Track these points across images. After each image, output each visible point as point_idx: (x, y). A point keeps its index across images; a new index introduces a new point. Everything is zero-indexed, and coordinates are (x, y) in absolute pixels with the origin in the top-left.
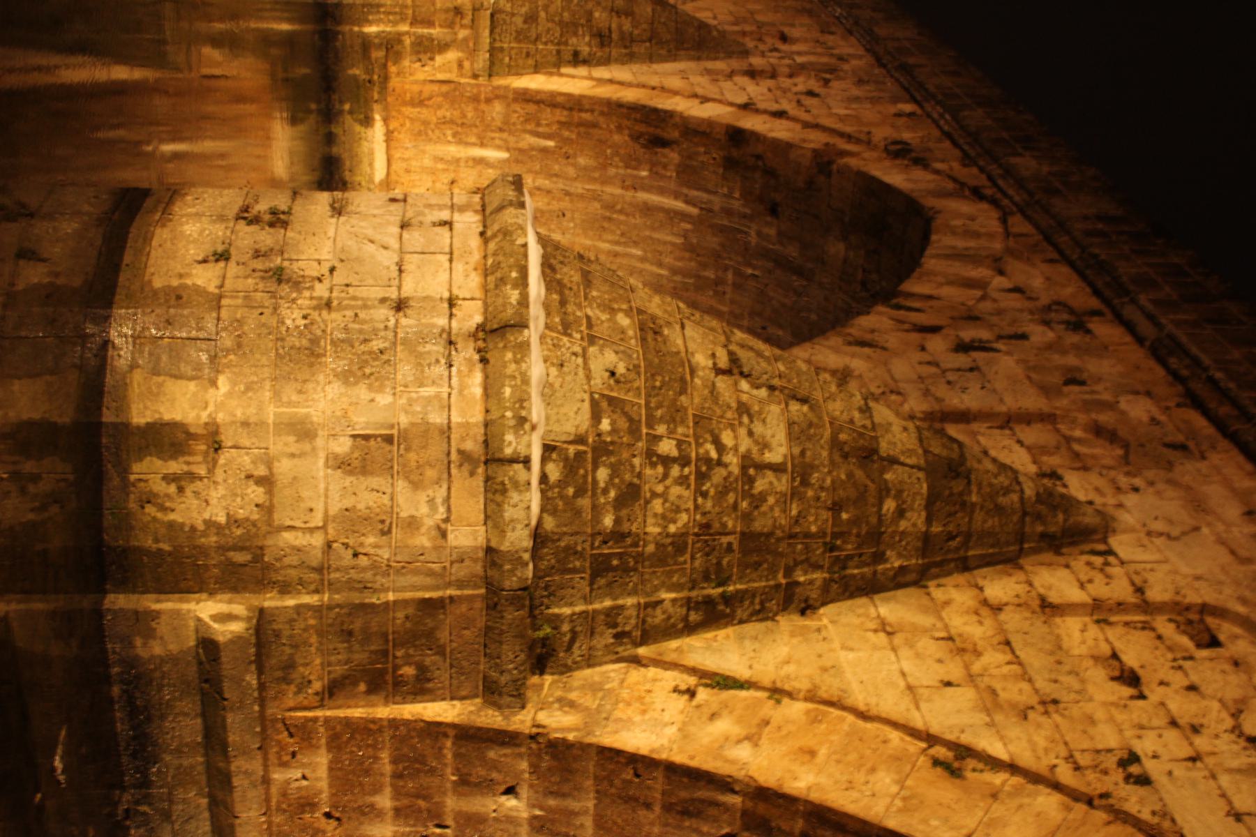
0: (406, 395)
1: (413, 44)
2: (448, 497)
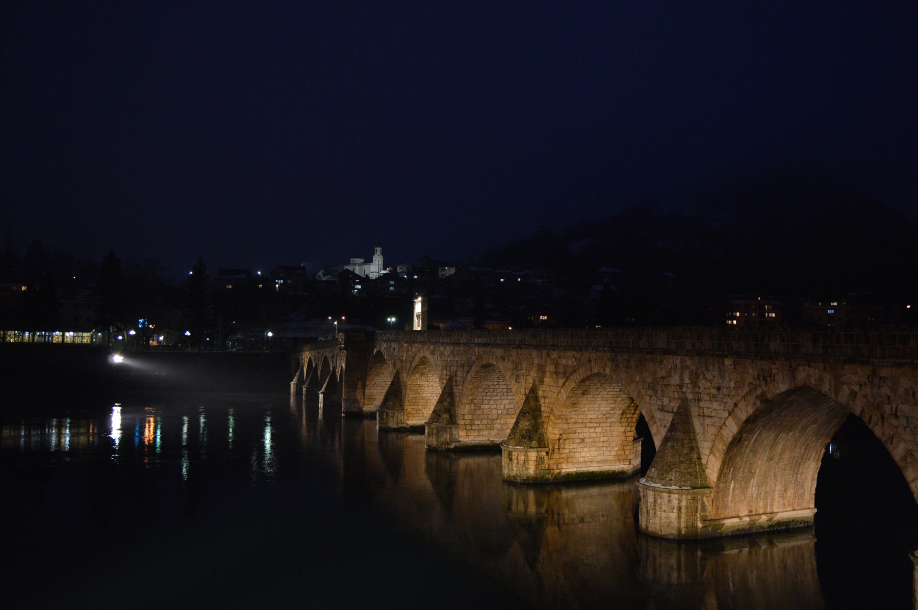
1: (703, 512)
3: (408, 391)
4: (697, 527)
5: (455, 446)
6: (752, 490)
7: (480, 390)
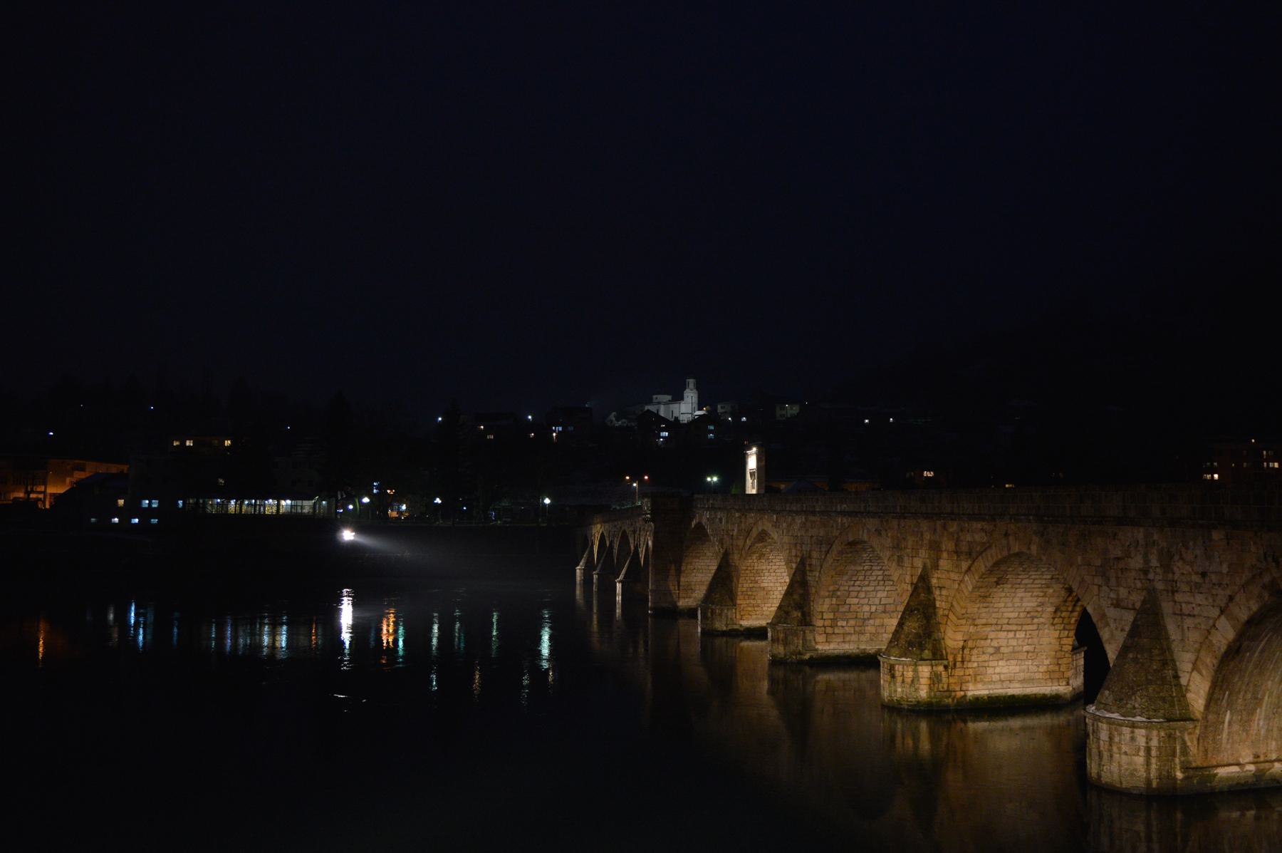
1: (1184, 756)
3: (741, 579)
4: (1175, 778)
5: (811, 658)
6: (1259, 721)
7: (845, 578)
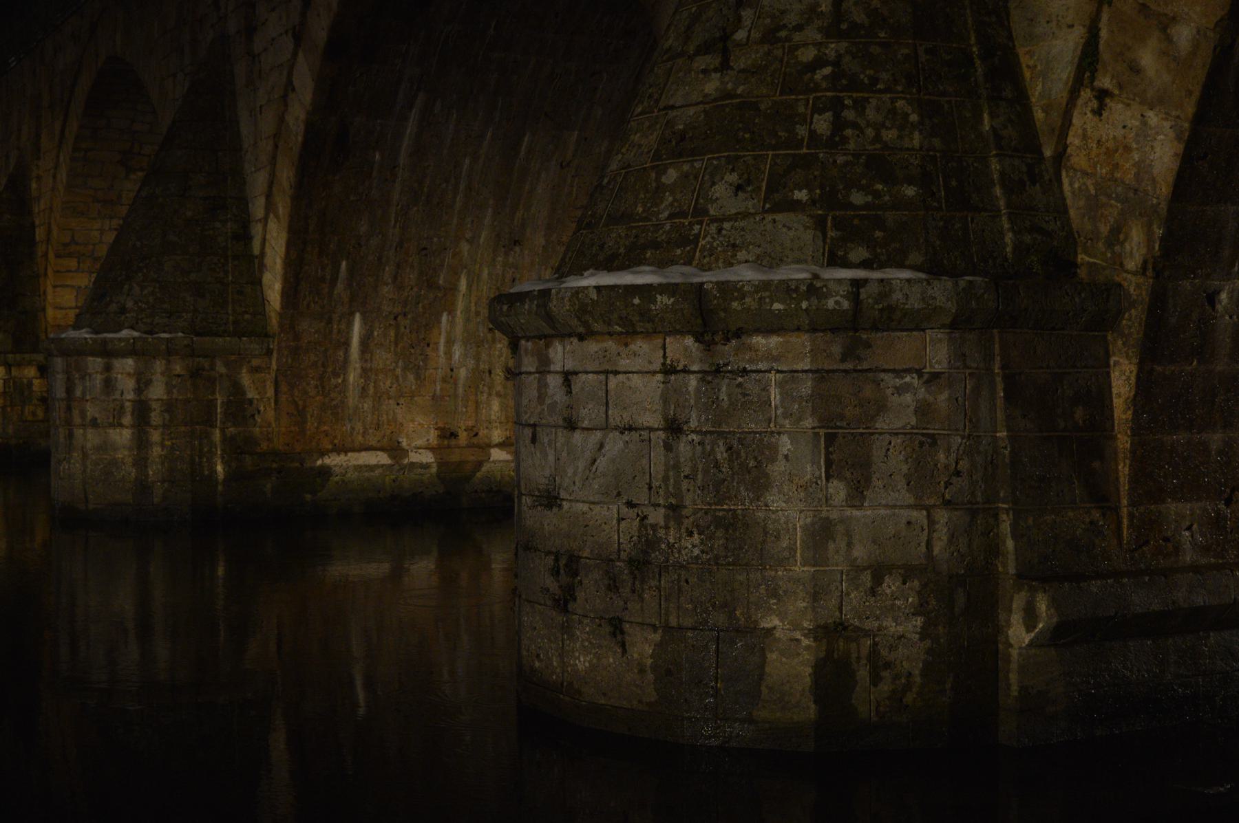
0: (780, 421)
2: (894, 371)
